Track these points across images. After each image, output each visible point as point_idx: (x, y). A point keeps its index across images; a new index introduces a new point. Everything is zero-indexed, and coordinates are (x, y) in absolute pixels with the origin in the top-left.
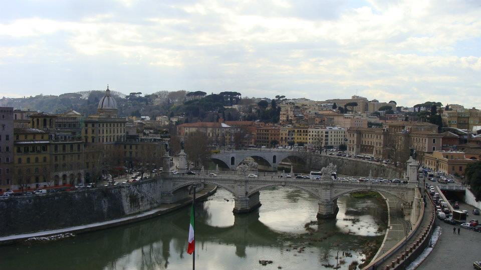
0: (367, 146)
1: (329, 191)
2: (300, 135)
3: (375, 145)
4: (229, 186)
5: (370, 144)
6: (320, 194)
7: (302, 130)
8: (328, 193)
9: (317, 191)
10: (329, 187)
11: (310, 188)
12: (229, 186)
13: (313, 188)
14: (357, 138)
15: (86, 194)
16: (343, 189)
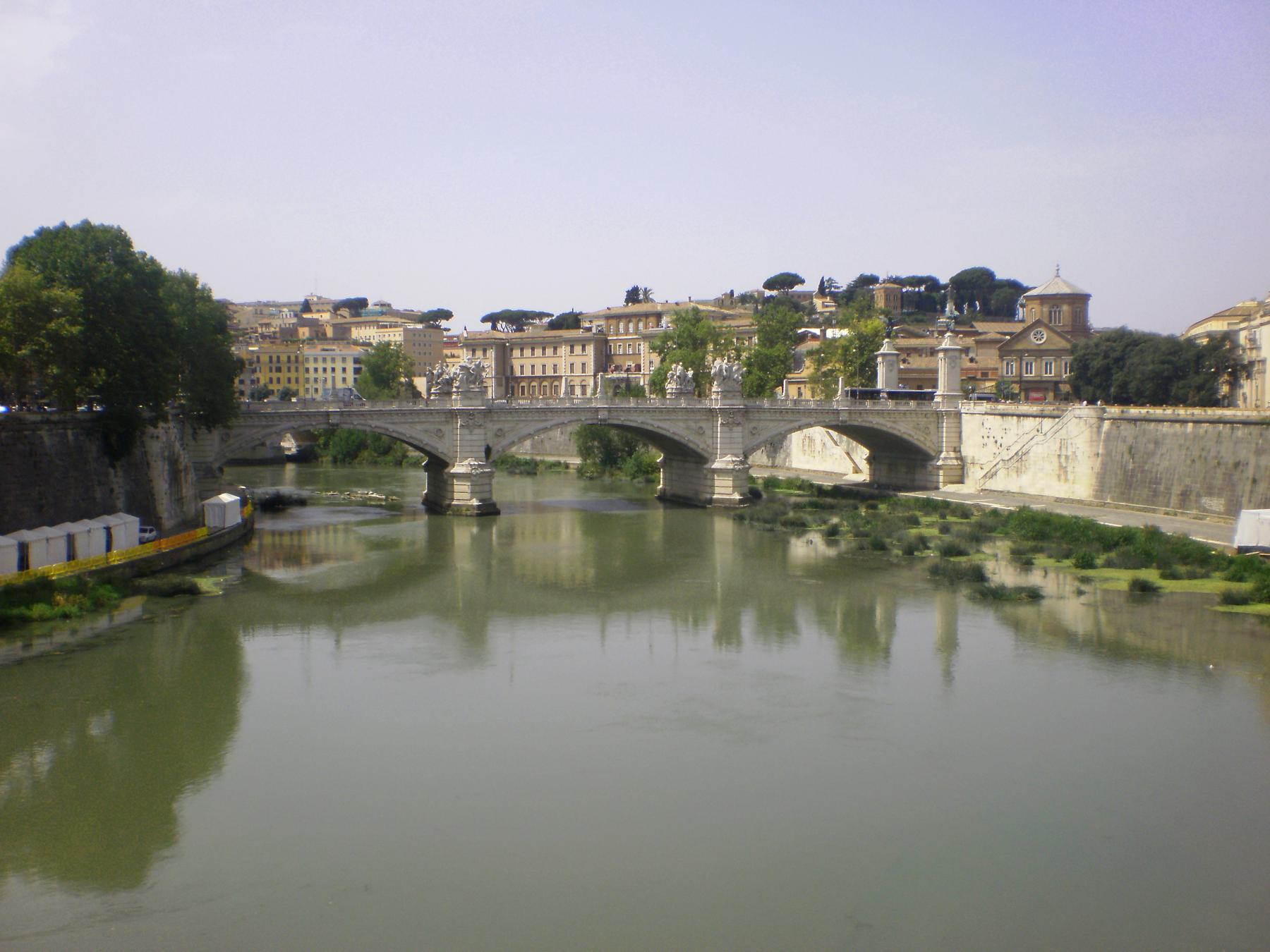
0: (532, 379)
1: (740, 429)
2: (279, 370)
3: (561, 372)
4: (426, 431)
5: (538, 373)
6: (709, 441)
7: (284, 358)
8: (735, 435)
9: (701, 432)
10: (739, 419)
11: (681, 424)
12: (426, 431)
13: (692, 424)
14: (496, 359)
15: (70, 432)
16: (771, 425)
